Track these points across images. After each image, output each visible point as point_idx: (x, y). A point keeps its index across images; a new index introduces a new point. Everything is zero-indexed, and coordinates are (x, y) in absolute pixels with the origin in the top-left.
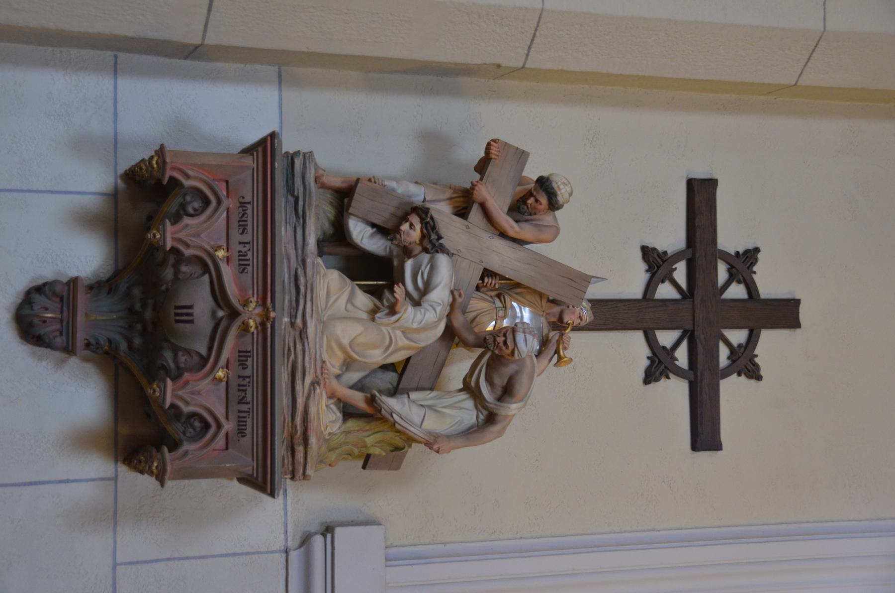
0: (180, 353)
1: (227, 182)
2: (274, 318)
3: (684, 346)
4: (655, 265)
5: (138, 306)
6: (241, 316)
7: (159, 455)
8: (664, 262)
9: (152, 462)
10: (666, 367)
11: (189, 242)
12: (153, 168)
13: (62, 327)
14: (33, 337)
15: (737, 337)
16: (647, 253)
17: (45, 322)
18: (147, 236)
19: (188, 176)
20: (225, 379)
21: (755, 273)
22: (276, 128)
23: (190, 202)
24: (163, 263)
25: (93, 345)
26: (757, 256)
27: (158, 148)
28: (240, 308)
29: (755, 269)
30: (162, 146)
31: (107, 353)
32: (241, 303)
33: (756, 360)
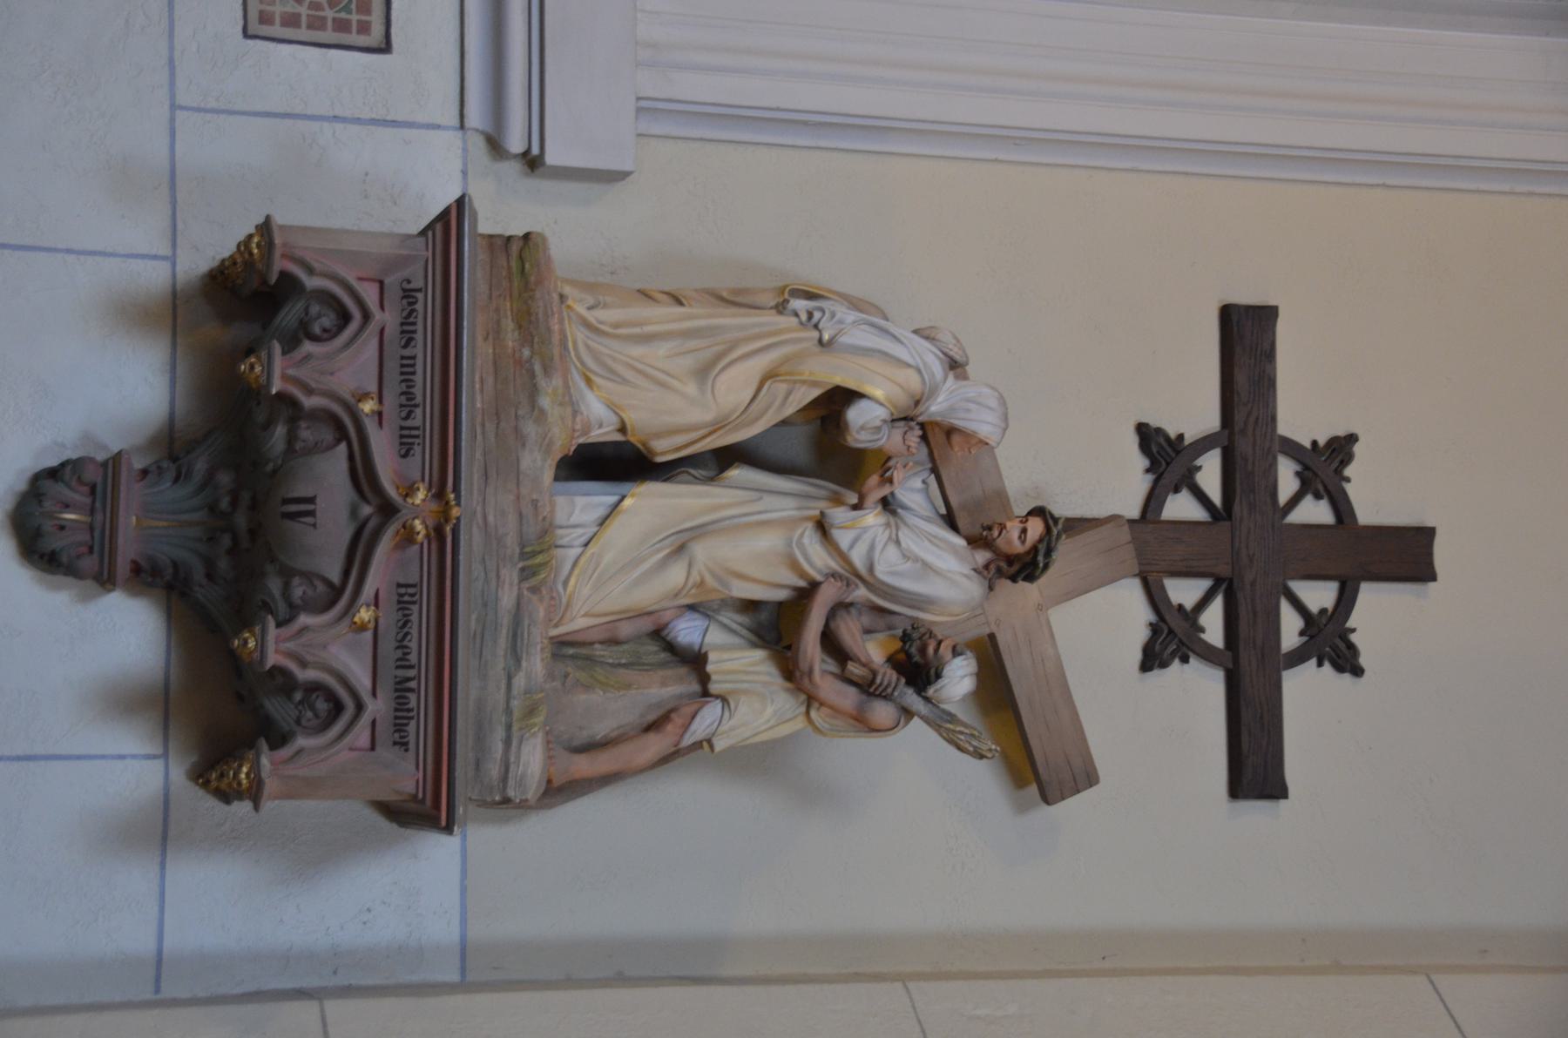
0: (296, 581)
1: (381, 283)
2: (458, 519)
5: (224, 504)
6: (399, 515)
8: (1178, 453)
11: (314, 385)
12: (251, 254)
13: (93, 537)
15: (1319, 596)
16: (1148, 437)
17: (62, 528)
19: (311, 271)
20: (372, 625)
21: (1348, 480)
23: (319, 316)
24: (268, 425)
26: (1351, 448)
27: (261, 220)
29: (1348, 472)
30: (268, 218)
31: (169, 587)
32: (400, 490)
33: (1354, 638)
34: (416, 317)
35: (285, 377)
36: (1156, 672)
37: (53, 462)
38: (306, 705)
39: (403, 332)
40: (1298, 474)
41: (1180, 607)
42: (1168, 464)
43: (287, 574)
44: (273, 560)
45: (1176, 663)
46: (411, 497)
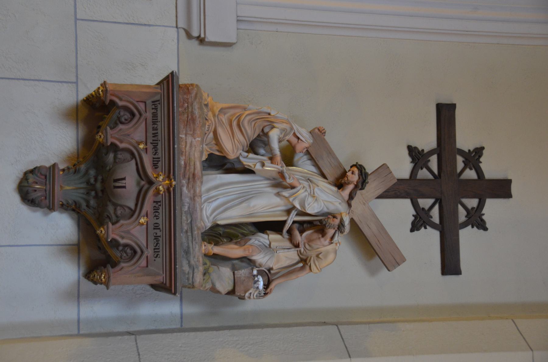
2: (175, 185)
3: (437, 207)
4: (417, 159)
5: (92, 181)
6: (154, 184)
9: (102, 274)
10: (424, 222)
12: (99, 94)
17: (35, 191)
20: (145, 224)
21: (481, 162)
22: (175, 69)
23: (124, 115)
24: (107, 154)
25: (65, 206)
28: (154, 179)
29: (481, 160)
33: (484, 217)
36: (416, 232)
37: (31, 167)
38: (123, 252)
41: (423, 209)
42: (418, 160)
43: (115, 205)
44: (110, 201)
45: (423, 228)
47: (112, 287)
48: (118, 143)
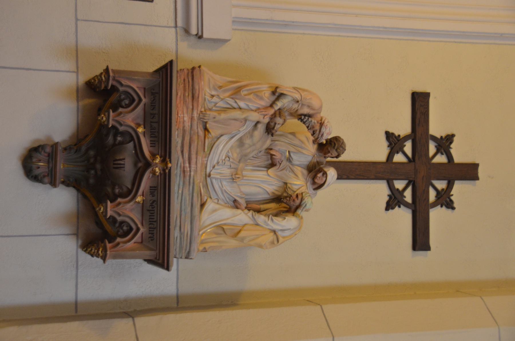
0: (117, 187)
2: (170, 168)
5: (92, 160)
7: (103, 245)
8: (398, 141)
9: (99, 249)
10: (398, 202)
12: (102, 79)
14: (32, 177)
15: (441, 185)
16: (389, 135)
18: (98, 118)
19: (122, 85)
20: (142, 202)
21: (451, 148)
22: (174, 58)
23: (124, 99)
24: (107, 135)
26: (453, 139)
27: (105, 68)
28: (151, 161)
29: (452, 146)
30: (107, 67)
32: (151, 158)
33: (452, 198)
34: (156, 101)
35: (113, 120)
36: (390, 211)
37: (36, 145)
39: (151, 106)
40: (436, 147)
41: (398, 189)
45: (397, 208)
46: (155, 161)
47: (109, 261)
48: (117, 125)
